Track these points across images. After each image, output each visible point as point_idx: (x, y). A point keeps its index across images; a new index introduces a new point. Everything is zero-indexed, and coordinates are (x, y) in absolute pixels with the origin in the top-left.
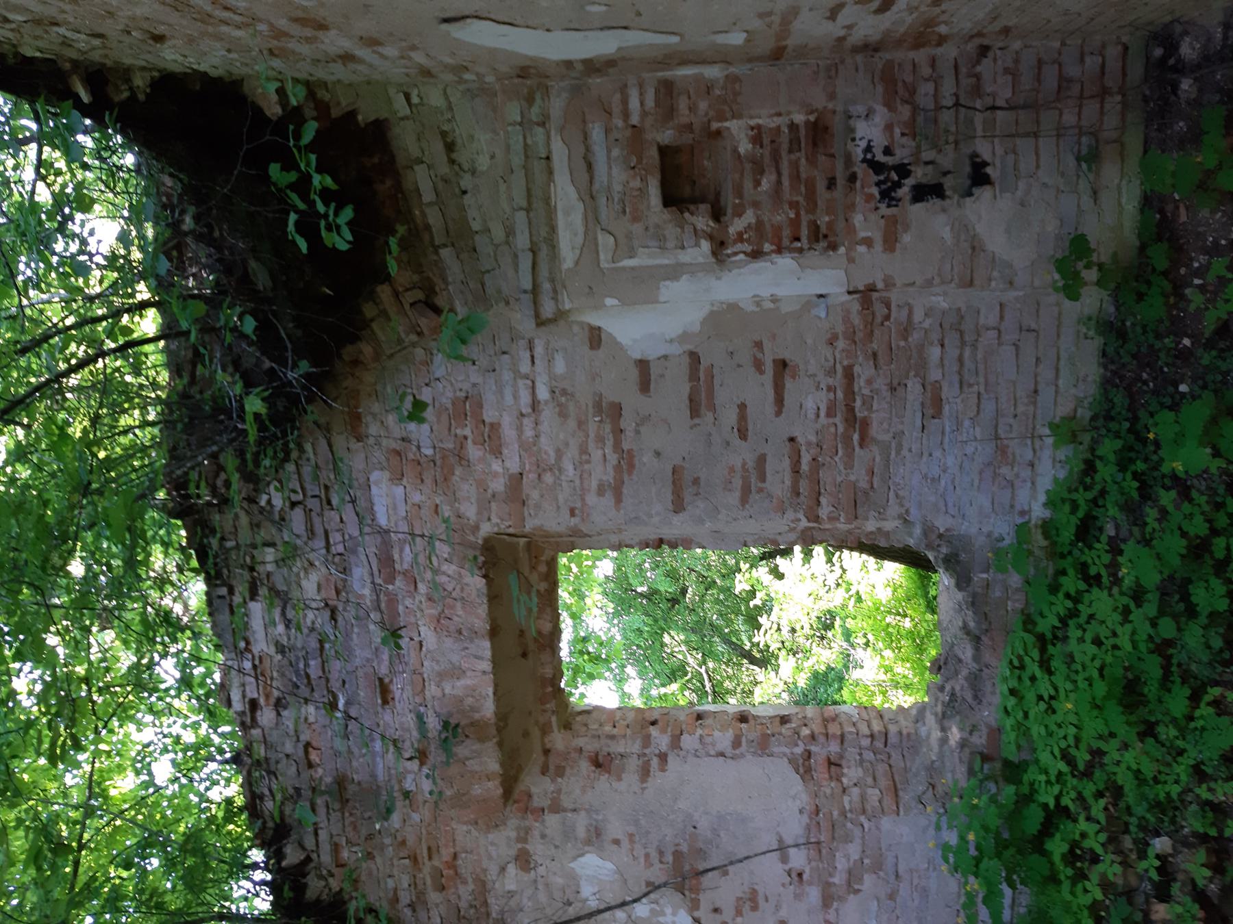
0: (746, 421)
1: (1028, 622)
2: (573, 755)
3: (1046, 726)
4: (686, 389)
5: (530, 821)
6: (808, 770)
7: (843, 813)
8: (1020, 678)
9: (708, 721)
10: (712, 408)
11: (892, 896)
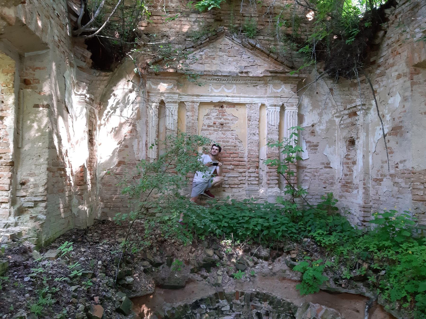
11: (393, 196)
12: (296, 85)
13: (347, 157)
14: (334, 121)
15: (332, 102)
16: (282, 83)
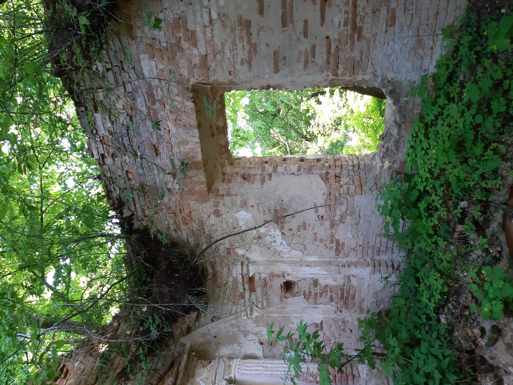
0: (307, 29)
1: (422, 118)
2: (234, 175)
3: (424, 160)
4: (280, 13)
5: (219, 199)
6: (327, 179)
7: (340, 195)
8: (415, 141)
9: (288, 161)
10: (292, 23)
11: (357, 224)
12: (199, 361)
13: (307, 296)
14: (256, 317)
15: (231, 320)
16: (192, 380)
